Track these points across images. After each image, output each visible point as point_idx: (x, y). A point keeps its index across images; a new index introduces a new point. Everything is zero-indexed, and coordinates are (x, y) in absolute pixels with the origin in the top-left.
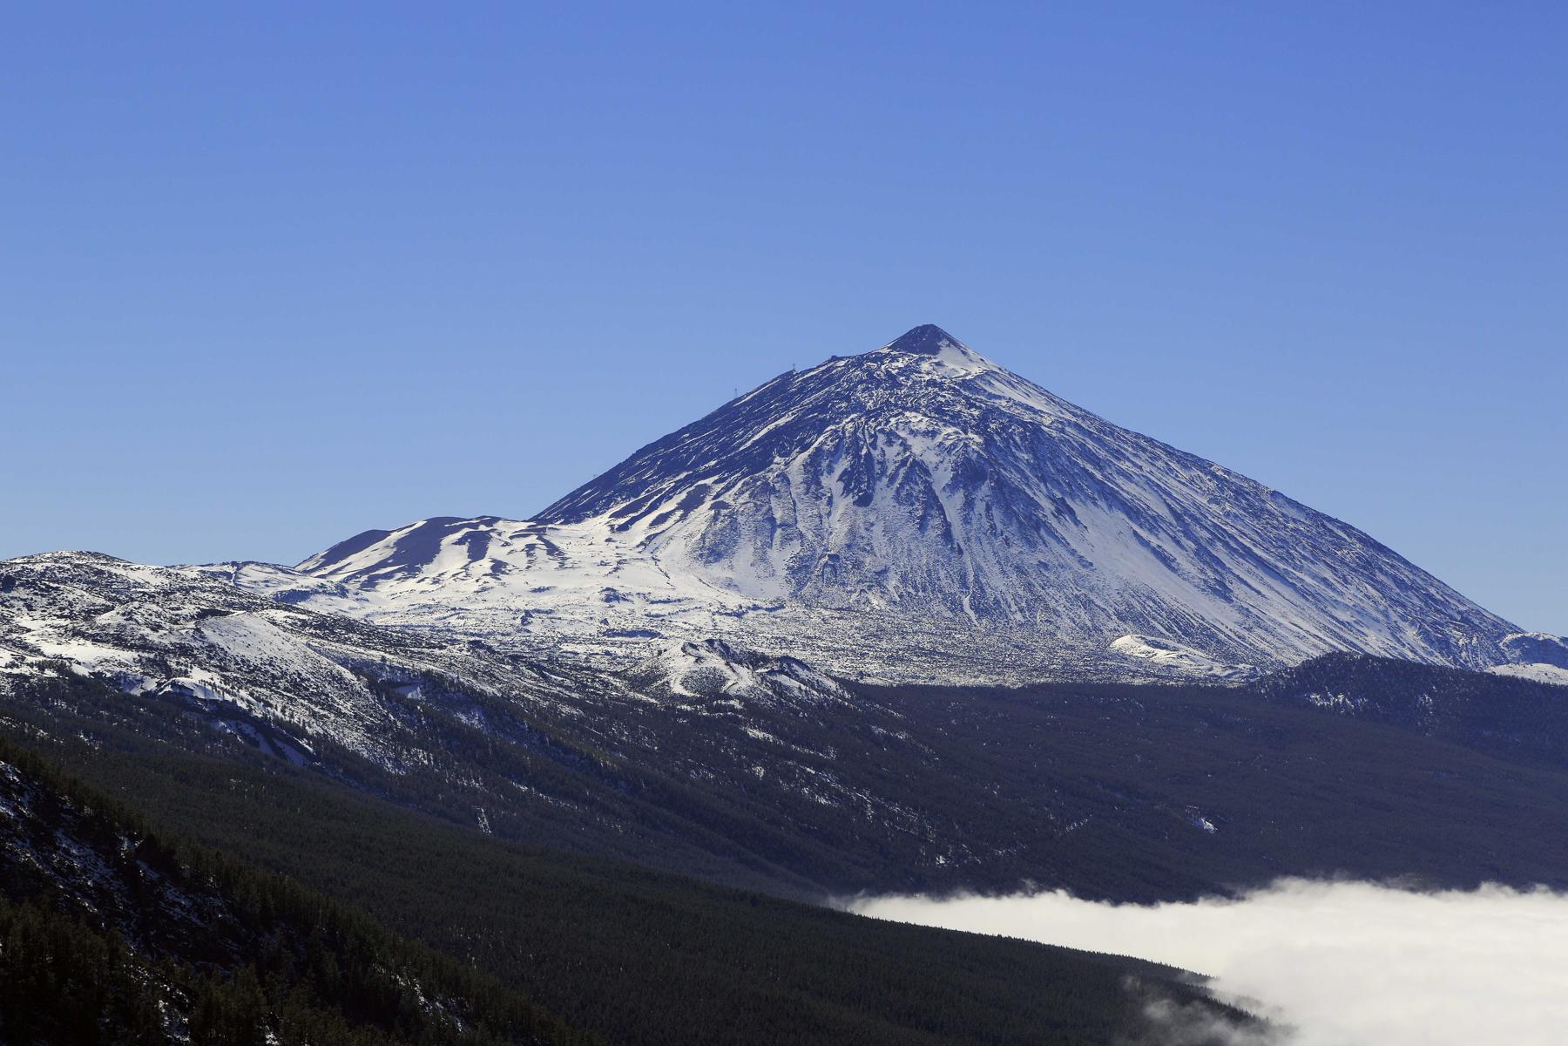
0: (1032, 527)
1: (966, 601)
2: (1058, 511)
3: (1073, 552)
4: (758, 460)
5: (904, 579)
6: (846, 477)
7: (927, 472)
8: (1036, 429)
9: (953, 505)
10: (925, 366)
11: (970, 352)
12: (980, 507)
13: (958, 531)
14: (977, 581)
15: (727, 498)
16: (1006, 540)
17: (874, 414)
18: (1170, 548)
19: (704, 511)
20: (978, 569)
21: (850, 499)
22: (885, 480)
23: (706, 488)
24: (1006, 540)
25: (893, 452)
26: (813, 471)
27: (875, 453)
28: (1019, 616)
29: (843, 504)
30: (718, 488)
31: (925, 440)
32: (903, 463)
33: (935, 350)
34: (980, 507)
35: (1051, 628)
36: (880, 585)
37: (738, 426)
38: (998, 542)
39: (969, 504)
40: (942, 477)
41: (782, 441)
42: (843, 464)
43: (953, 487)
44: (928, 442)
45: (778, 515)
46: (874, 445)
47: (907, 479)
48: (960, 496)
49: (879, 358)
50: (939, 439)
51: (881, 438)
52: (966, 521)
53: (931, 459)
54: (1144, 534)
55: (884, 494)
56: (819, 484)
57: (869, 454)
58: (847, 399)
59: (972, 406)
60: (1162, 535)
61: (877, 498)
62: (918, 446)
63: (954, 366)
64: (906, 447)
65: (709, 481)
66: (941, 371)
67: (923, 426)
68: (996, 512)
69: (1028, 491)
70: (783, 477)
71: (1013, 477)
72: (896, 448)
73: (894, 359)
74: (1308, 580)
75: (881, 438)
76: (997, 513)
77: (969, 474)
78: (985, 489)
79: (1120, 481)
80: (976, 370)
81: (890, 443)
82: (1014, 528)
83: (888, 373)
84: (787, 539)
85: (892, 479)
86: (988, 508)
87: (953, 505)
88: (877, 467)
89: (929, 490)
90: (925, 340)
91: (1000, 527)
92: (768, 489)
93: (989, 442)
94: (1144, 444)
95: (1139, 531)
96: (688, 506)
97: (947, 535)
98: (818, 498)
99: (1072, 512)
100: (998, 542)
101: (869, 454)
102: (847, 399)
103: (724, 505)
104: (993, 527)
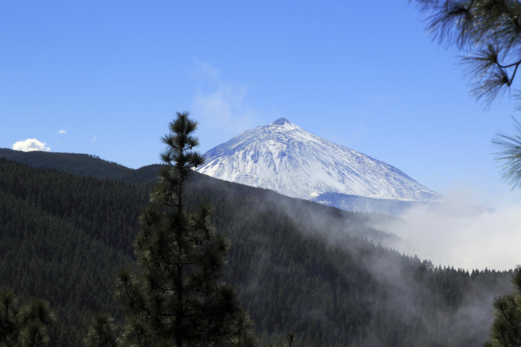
0: (296, 167)
1: (277, 185)
2: (304, 163)
3: (306, 173)
4: (232, 152)
5: (263, 180)
6: (253, 156)
7: (272, 154)
8: (301, 143)
9: (277, 162)
10: (279, 128)
11: (292, 124)
12: (284, 162)
13: (277, 168)
14: (280, 180)
15: (223, 162)
16: (289, 171)
17: (261, 140)
18: (331, 171)
19: (217, 165)
20: (281, 177)
21: (253, 161)
22: (261, 157)
23: (219, 160)
24: (289, 171)
25: (264, 150)
26: (245, 155)
27: (260, 150)
28: (289, 188)
29: (251, 162)
30: (221, 160)
31: (274, 147)
32: (266, 152)
33: (283, 124)
34: (284, 162)
35: (296, 191)
36: (256, 182)
37: (231, 144)
38: (287, 171)
39: (281, 162)
40: (275, 155)
41: (238, 148)
42: (252, 153)
43: (278, 158)
44: (273, 147)
45: (235, 166)
46: (260, 148)
47: (267, 156)
48: (279, 160)
49: (268, 126)
50: (276, 146)
51: (262, 146)
52: (280, 166)
53: (273, 151)
54: (325, 168)
55: (261, 159)
56: (245, 158)
57: (258, 150)
58: (257, 137)
59: (286, 138)
60: (330, 168)
61: (259, 161)
62: (270, 148)
63: (287, 127)
64: (267, 148)
65: (220, 158)
66: (283, 129)
67: (273, 143)
68: (288, 164)
69: (296, 158)
70: (238, 157)
71: (293, 155)
72: (265, 149)
73: (272, 126)
74: (368, 178)
75: (262, 146)
76: (288, 164)
77: (282, 154)
78: (285, 158)
79: (322, 155)
80: (292, 129)
81: (264, 147)
82: (292, 167)
83: (269, 131)
84: (236, 171)
85: (263, 156)
86: (286, 163)
87: (277, 162)
88: (260, 154)
89: (272, 159)
90: (280, 122)
91: (288, 167)
92: (233, 159)
93: (288, 147)
94: (335, 146)
95: (324, 167)
96: (214, 164)
97: (275, 169)
98: (245, 161)
99: (307, 163)
100: (287, 171)
101: (258, 150)
102: (257, 137)
103: (222, 164)
104: (286, 167)
